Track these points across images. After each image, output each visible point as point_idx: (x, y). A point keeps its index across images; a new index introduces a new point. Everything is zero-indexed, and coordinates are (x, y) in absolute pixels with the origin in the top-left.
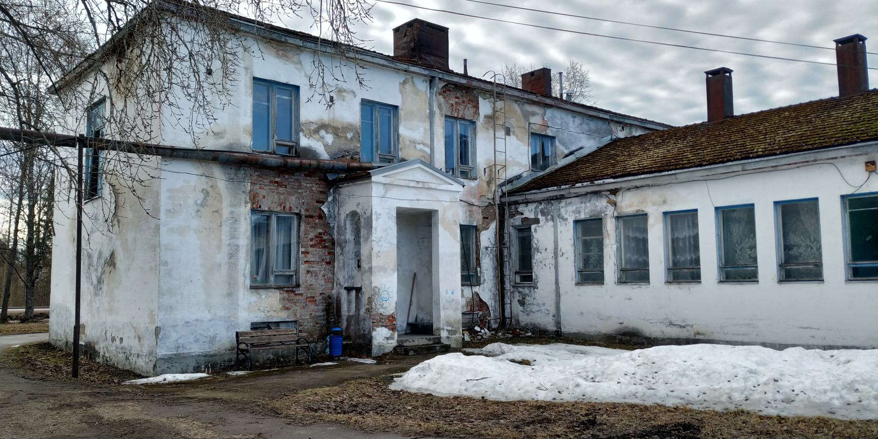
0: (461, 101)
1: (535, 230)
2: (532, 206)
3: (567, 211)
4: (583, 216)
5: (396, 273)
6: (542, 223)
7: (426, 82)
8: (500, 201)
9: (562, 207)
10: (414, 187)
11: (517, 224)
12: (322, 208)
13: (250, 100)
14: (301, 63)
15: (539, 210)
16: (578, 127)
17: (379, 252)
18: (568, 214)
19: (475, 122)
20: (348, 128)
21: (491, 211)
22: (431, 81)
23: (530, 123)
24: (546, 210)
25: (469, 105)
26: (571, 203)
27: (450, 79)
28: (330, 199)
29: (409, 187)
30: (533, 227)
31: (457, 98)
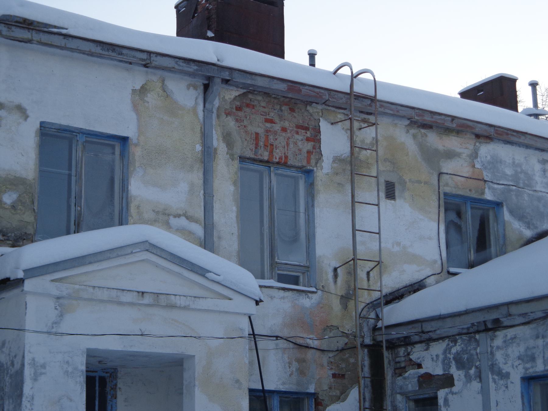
0: (277, 127)
1: (446, 401)
2: (438, 348)
3: (507, 355)
6: (458, 385)
7: (195, 88)
8: (374, 340)
9: (498, 348)
10: (131, 304)
11: (410, 388)
15: (452, 356)
18: (510, 363)
21: (352, 360)
22: (206, 87)
23: (440, 174)
24: (466, 356)
25: (297, 136)
26: (514, 338)
27: (249, 82)
29: (121, 303)
30: (442, 394)
31: (267, 121)
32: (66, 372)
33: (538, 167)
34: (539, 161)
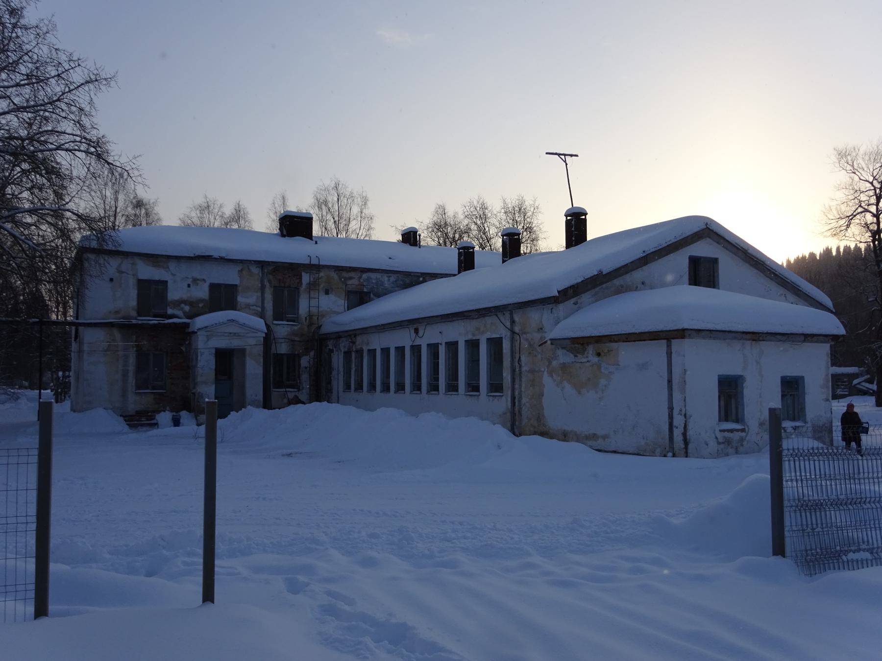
2: (332, 341)
4: (346, 350)
5: (214, 386)
12: (182, 348)
13: (136, 292)
14: (168, 268)
16: (393, 283)
17: (202, 373)
19: (298, 289)
20: (202, 300)
22: (262, 267)
23: (346, 285)
28: (187, 343)
30: (332, 354)
31: (284, 274)
32: (210, 354)
33: (386, 279)
34: (387, 277)
